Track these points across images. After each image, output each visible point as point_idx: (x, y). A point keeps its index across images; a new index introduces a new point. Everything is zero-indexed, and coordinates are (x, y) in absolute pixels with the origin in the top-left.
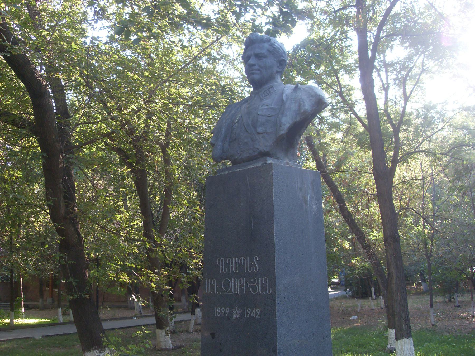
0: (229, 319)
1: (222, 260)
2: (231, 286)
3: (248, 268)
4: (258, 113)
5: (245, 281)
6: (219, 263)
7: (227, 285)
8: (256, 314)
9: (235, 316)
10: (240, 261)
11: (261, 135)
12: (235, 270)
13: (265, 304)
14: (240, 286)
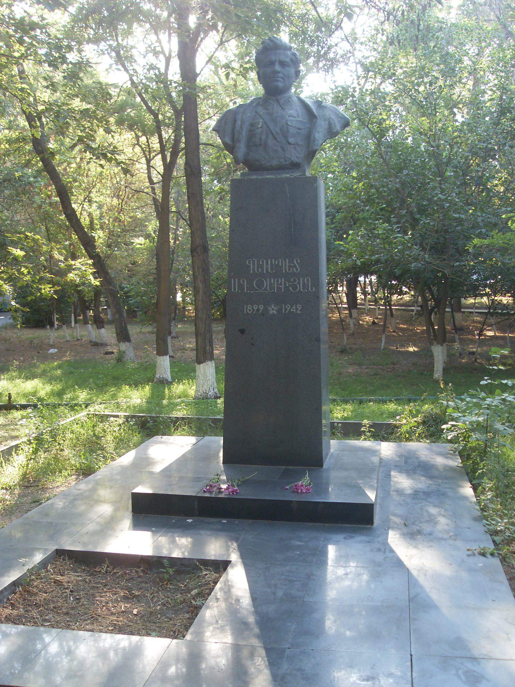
0: (263, 315)
1: (254, 261)
2: (265, 285)
3: (287, 269)
4: (289, 124)
6: (249, 263)
7: (260, 284)
8: (297, 309)
9: (271, 312)
11: (292, 146)
12: (271, 270)
14: (277, 285)
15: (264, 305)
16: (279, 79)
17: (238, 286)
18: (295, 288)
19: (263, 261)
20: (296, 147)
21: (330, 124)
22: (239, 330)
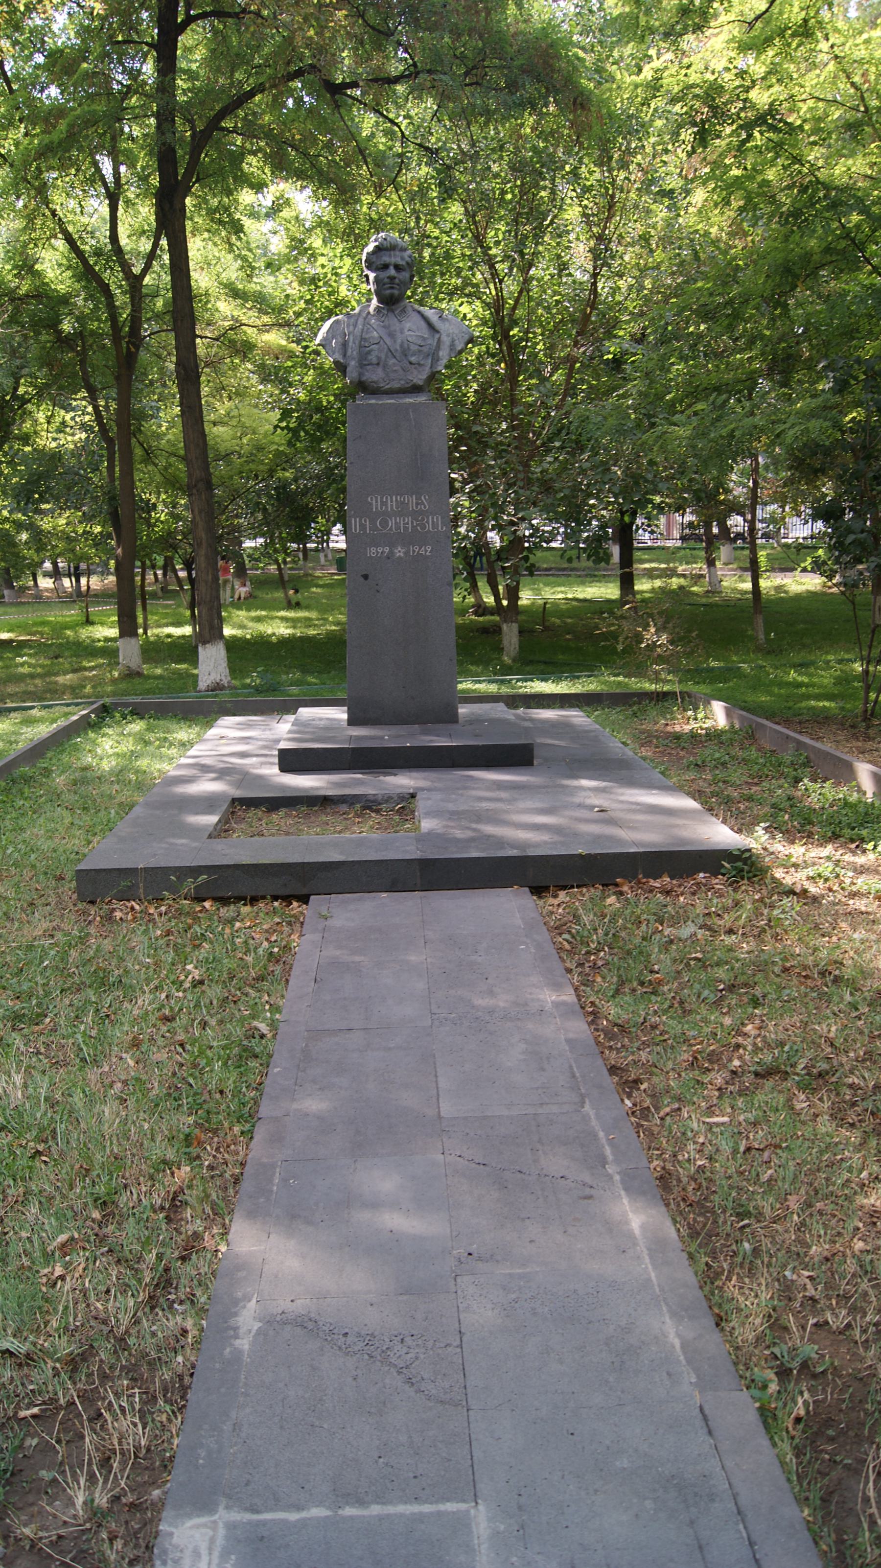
7: (384, 523)
18: (423, 527)
21: (453, 341)
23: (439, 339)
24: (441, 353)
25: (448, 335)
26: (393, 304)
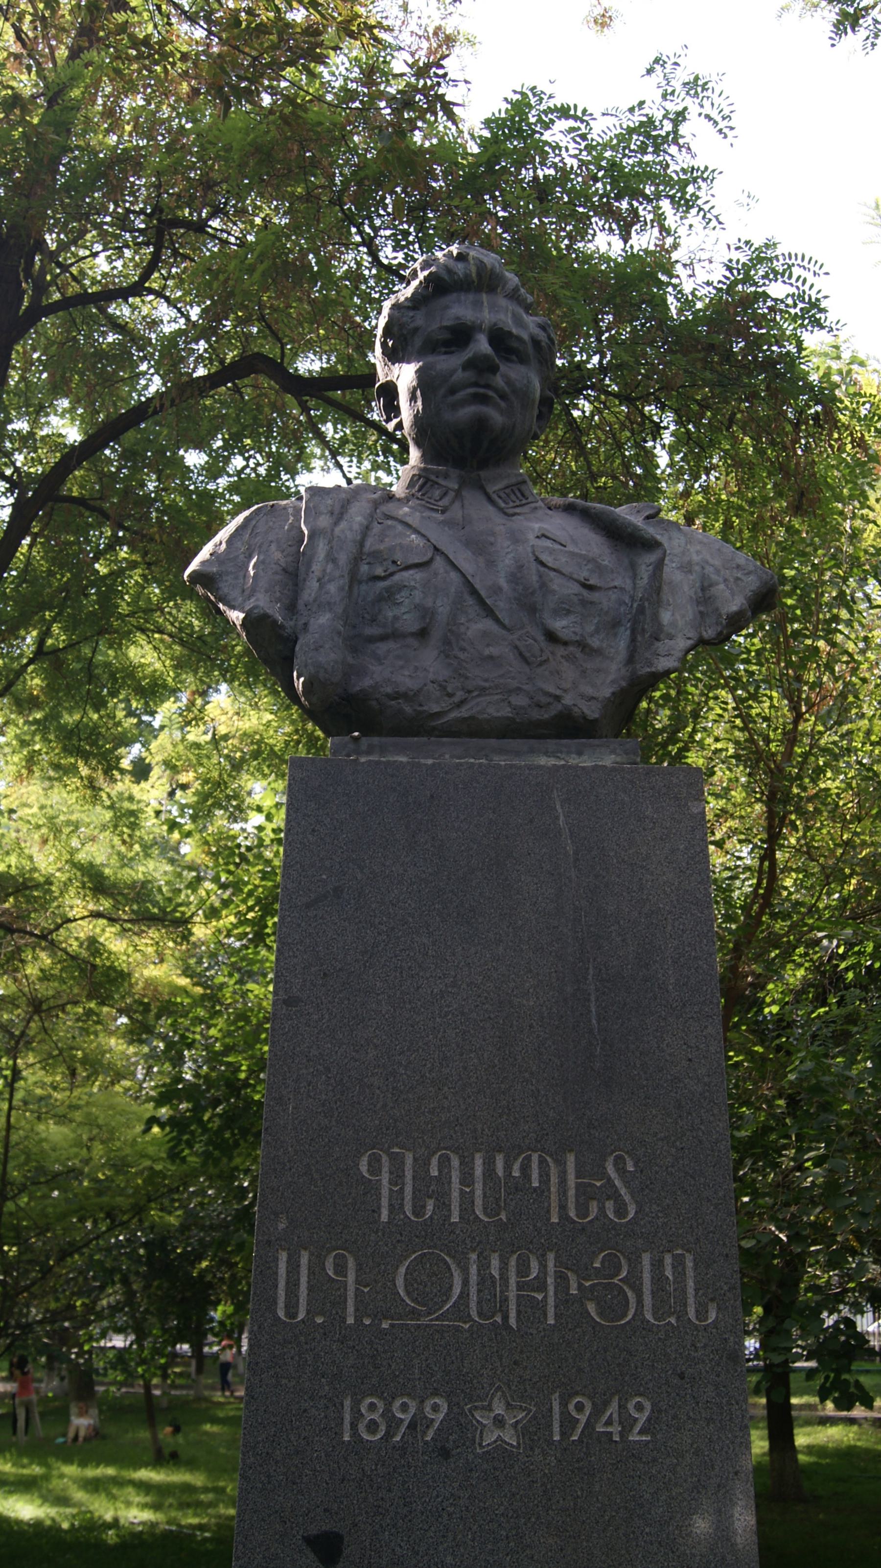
0: (445, 1453)
2: (457, 1290)
5: (551, 1264)
6: (375, 1169)
8: (627, 1423)
10: (516, 1167)
11: (561, 651)
12: (485, 1210)
13: (682, 1376)
14: (520, 1287)
15: (448, 1397)
16: (491, 393)
17: (310, 1289)
19: (444, 1162)
20: (579, 655)
21: (705, 586)
22: (310, 1541)
23: (659, 565)
24: (666, 617)
25: (687, 568)
26: (483, 464)
